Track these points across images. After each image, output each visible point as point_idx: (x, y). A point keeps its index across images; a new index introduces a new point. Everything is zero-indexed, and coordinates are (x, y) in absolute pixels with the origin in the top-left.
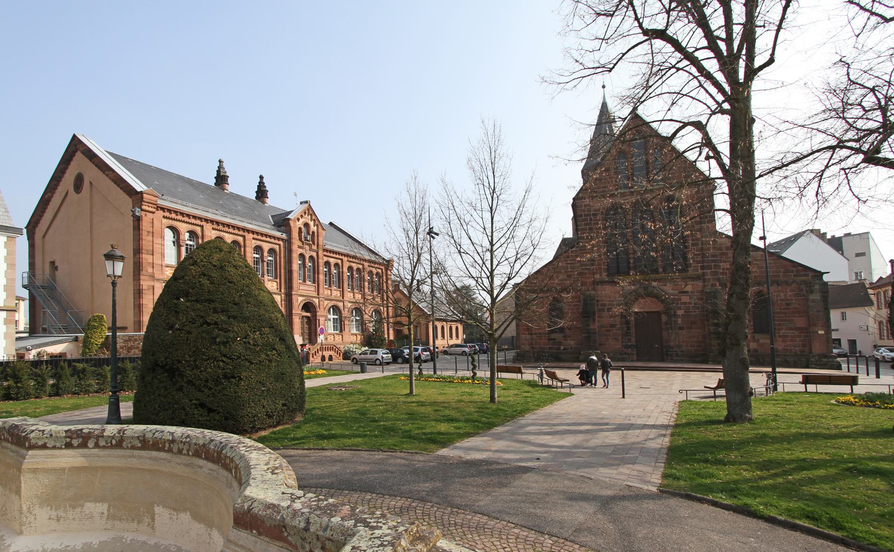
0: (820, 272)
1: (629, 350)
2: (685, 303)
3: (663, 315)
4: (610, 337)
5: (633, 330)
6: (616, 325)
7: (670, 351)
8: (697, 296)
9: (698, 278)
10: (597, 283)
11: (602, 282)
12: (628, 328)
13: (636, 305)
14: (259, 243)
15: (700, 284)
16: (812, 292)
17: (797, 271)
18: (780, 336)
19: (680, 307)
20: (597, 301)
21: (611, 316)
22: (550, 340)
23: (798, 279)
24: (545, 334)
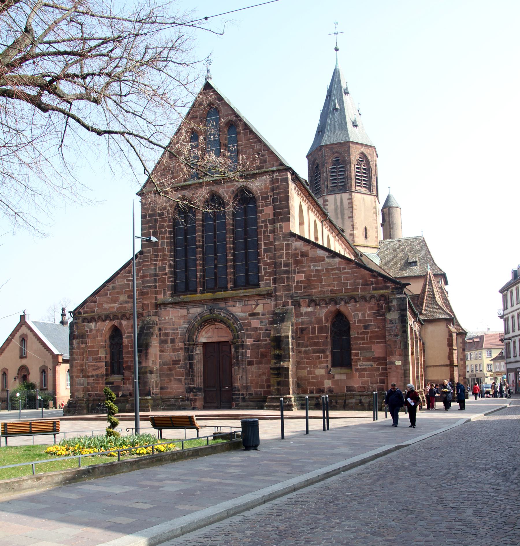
1: (191, 395)
2: (255, 329)
6: (180, 361)
8: (268, 318)
9: (269, 295)
10: (160, 304)
11: (165, 304)
12: (191, 365)
13: (204, 333)
15: (271, 302)
16: (389, 310)
17: (377, 283)
18: (357, 370)
19: (250, 334)
21: (174, 350)
23: (377, 293)
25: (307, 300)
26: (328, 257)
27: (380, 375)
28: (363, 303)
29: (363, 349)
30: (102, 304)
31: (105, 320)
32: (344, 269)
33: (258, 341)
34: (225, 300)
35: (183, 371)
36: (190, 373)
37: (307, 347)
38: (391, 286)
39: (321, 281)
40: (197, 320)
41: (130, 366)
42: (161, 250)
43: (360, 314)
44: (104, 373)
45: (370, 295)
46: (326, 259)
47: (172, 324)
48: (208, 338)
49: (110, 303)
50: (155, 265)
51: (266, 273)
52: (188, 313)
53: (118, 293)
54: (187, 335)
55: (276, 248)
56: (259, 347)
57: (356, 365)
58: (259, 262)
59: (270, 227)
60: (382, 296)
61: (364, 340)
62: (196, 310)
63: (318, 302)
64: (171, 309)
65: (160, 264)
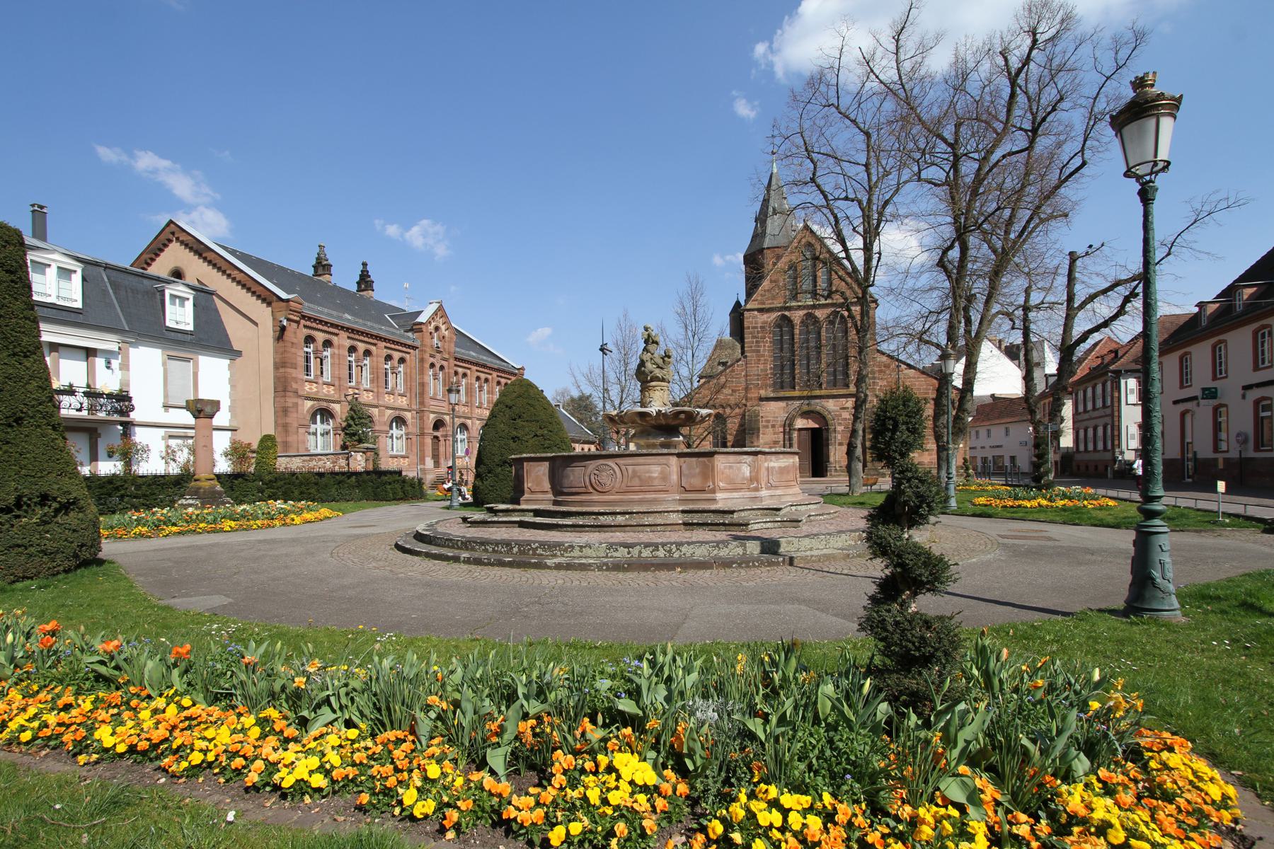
14: (390, 352)
42: (763, 356)
65: (761, 367)
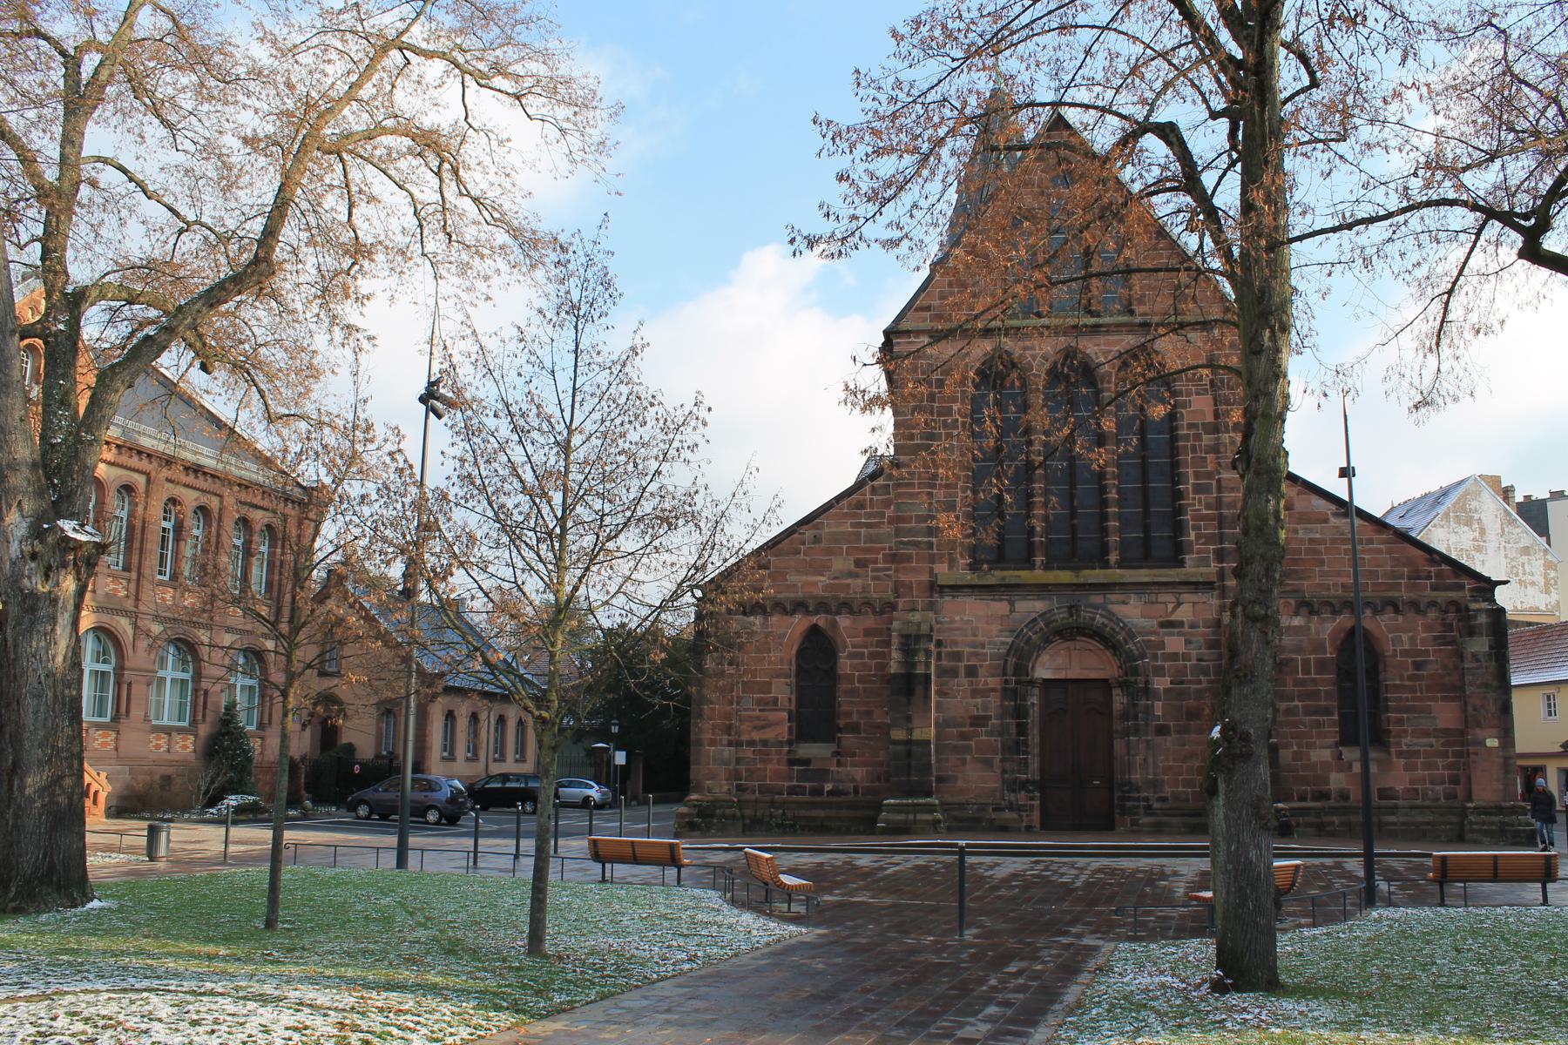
0: (1488, 580)
1: (1021, 798)
2: (1174, 656)
3: (1116, 692)
4: (968, 757)
5: (1034, 737)
6: (989, 718)
7: (1129, 799)
10: (942, 587)
11: (956, 589)
12: (1022, 729)
18: (1400, 754)
19: (1162, 668)
20: (939, 643)
21: (975, 693)
22: (791, 762)
24: (781, 743)
25: (1293, 602)
26: (1336, 515)
27: (1449, 767)
28: (1411, 615)
29: (1413, 709)
30: (784, 575)
31: (793, 613)
32: (1370, 541)
33: (1182, 682)
34: (1105, 587)
35: (997, 741)
36: (1016, 747)
37: (1293, 700)
38: (1468, 584)
39: (1322, 563)
40: (1037, 628)
41: (858, 724)
43: (1405, 637)
44: (786, 737)
45: (1426, 600)
46: (1332, 519)
47: (970, 632)
48: (1057, 669)
49: (807, 574)
50: (930, 495)
51: (1198, 537)
52: (1012, 611)
53: (829, 552)
54: (1012, 661)
55: (1224, 484)
56: (1182, 695)
57: (1399, 744)
58: (1179, 511)
59: (1207, 439)
60: (1453, 603)
61: (1415, 692)
62: (1032, 607)
63: (1316, 607)
64: (967, 599)
